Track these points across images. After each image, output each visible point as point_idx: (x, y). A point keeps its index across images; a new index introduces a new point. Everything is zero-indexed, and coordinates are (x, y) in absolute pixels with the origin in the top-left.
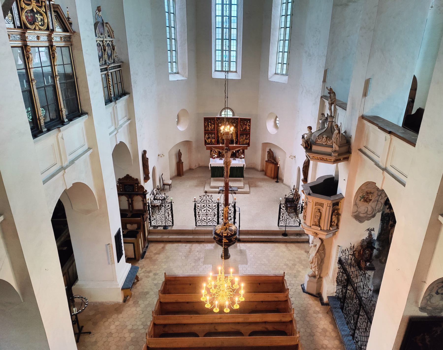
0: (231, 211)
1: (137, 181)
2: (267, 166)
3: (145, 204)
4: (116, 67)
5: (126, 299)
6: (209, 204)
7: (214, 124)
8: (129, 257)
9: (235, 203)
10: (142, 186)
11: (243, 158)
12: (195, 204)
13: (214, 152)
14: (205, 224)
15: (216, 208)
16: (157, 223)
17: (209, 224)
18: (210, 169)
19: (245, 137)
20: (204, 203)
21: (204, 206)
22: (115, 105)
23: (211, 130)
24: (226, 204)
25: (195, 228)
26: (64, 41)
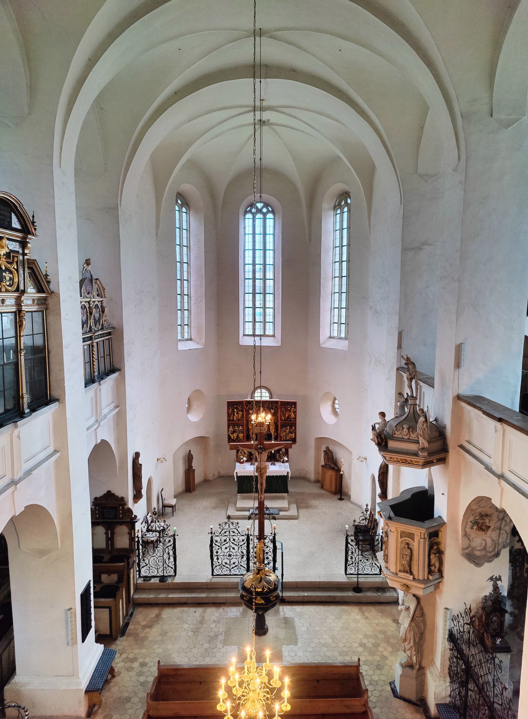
0: (268, 549)
1: (122, 501)
2: (324, 474)
3: (132, 539)
4: (105, 335)
5: (92, 710)
6: (234, 537)
7: (242, 411)
8: (102, 633)
9: (275, 534)
10: (129, 508)
11: (287, 461)
12: (212, 537)
13: (241, 453)
14: (228, 573)
15: (244, 544)
16: (150, 572)
17: (233, 572)
18: (236, 480)
19: (288, 429)
20: (226, 536)
21: (225, 541)
22: (98, 387)
23: (238, 420)
24: (261, 536)
25: (211, 580)
26: (38, 304)
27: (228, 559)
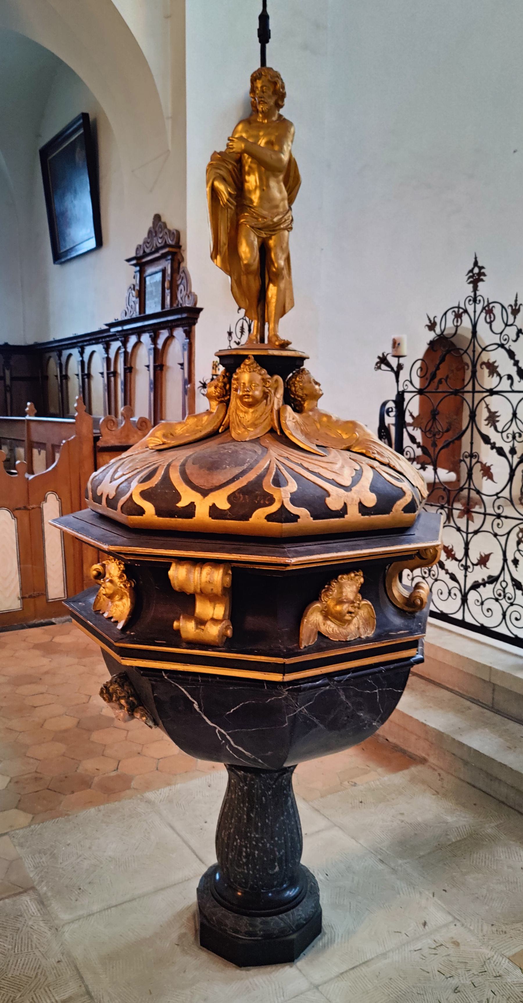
27: (459, 529)
